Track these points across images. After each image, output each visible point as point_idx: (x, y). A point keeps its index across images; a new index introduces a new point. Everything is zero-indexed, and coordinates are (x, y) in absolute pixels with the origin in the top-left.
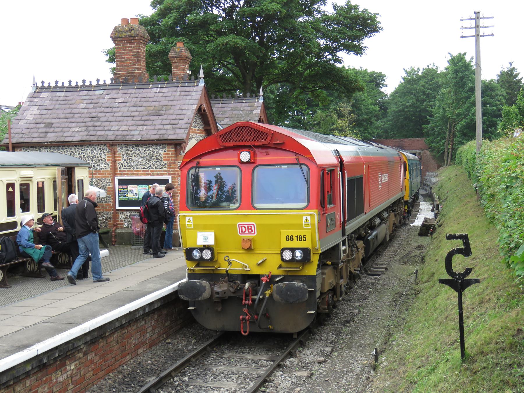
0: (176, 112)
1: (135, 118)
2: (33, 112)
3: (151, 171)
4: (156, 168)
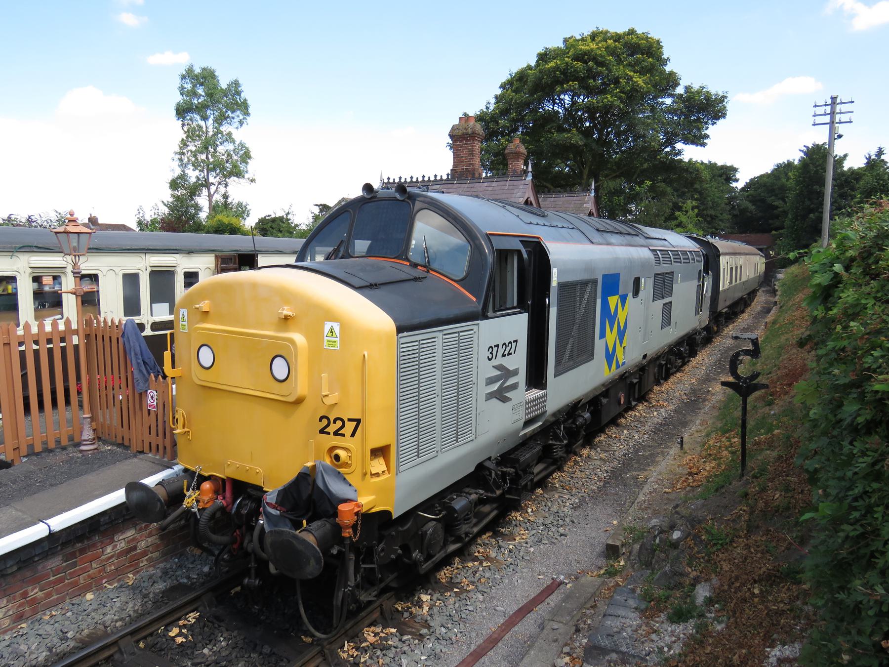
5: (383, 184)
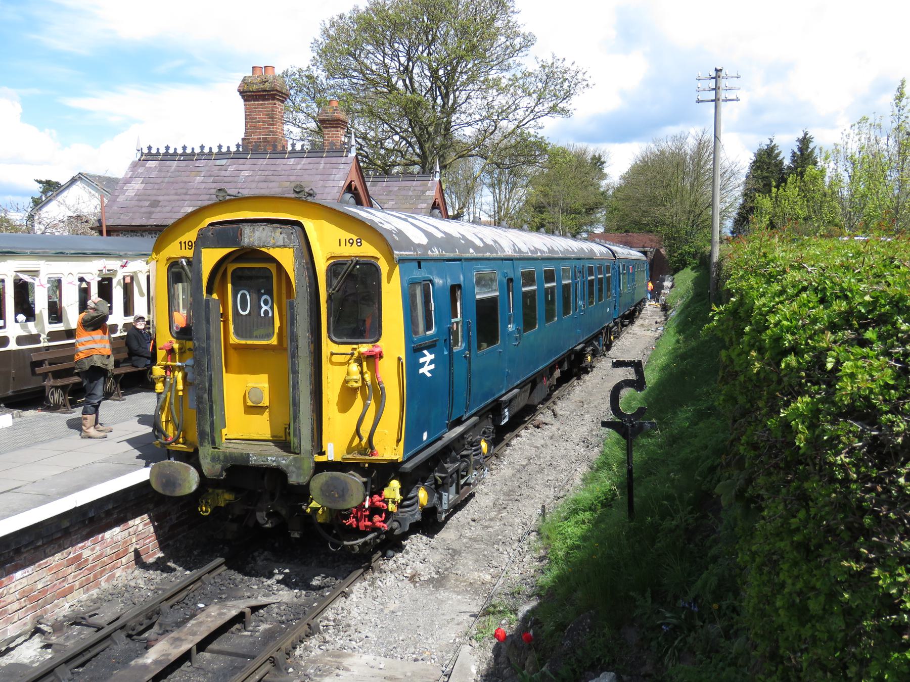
2: (137, 185)
5: (142, 155)
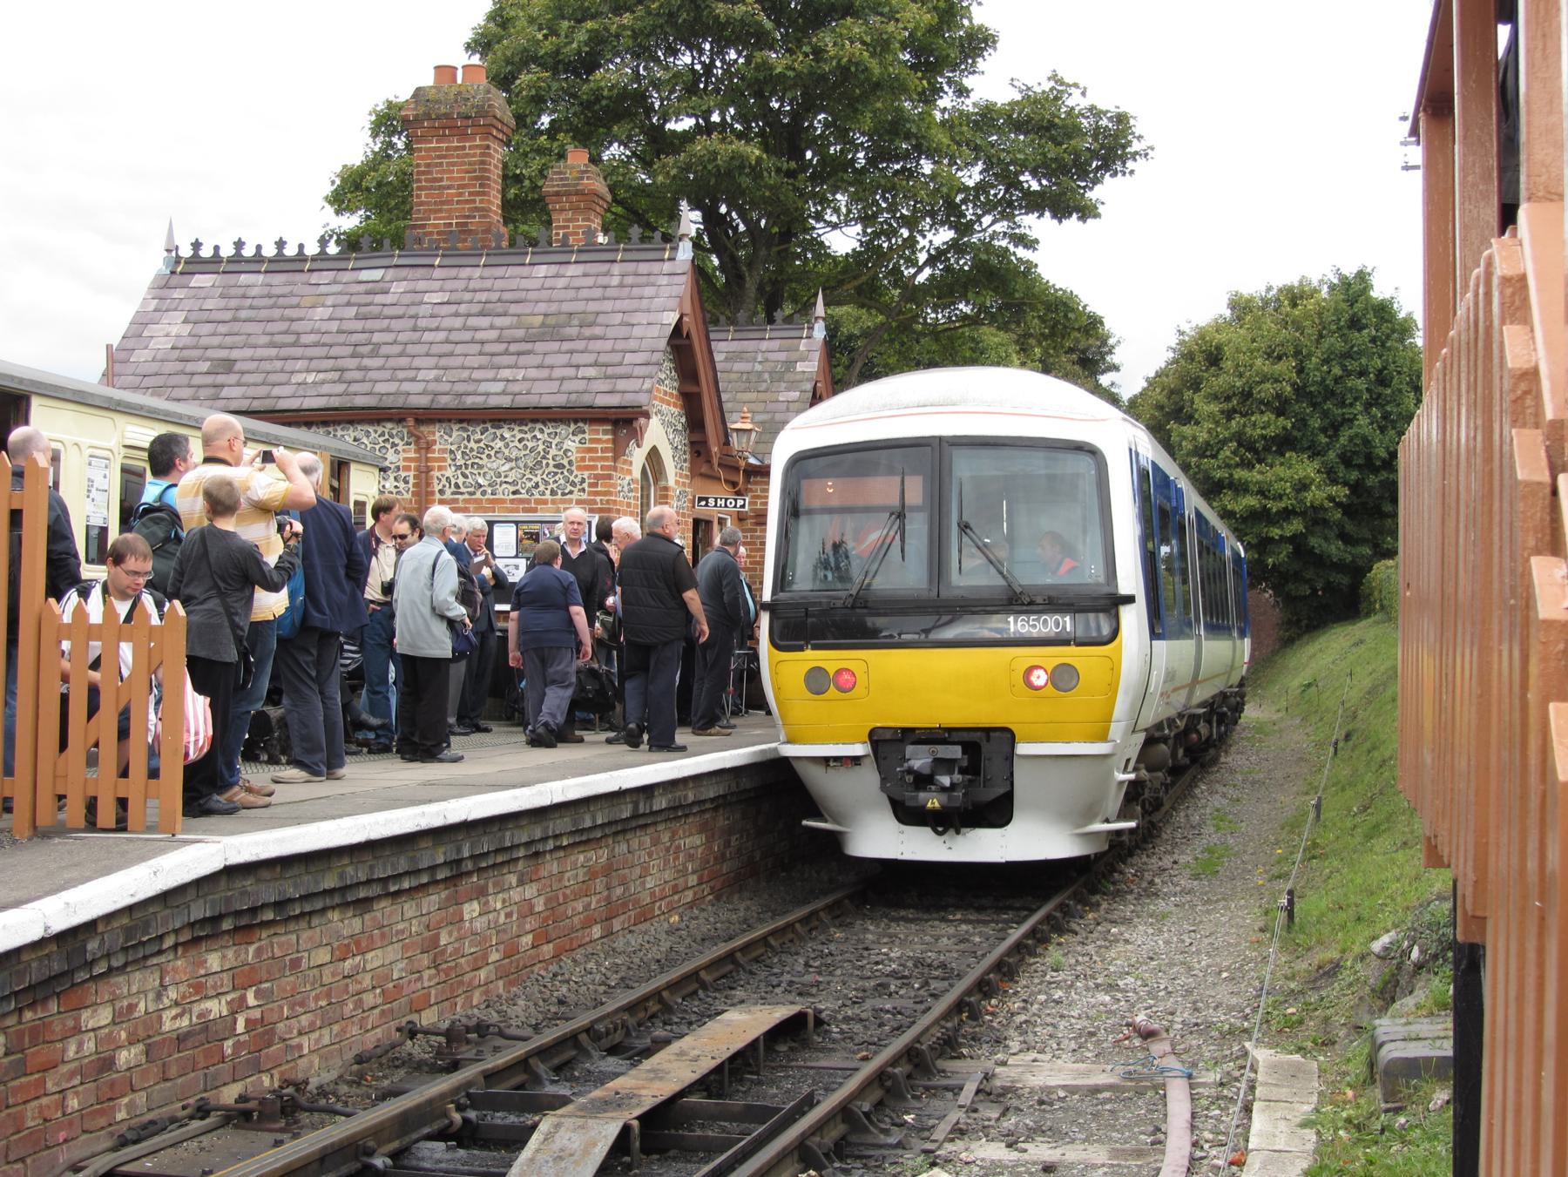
0: (611, 332)
1: (488, 348)
3: (538, 502)
4: (553, 493)
